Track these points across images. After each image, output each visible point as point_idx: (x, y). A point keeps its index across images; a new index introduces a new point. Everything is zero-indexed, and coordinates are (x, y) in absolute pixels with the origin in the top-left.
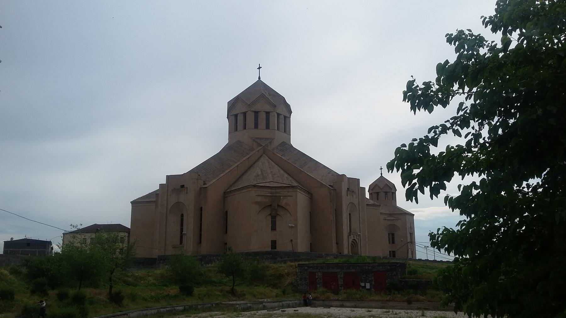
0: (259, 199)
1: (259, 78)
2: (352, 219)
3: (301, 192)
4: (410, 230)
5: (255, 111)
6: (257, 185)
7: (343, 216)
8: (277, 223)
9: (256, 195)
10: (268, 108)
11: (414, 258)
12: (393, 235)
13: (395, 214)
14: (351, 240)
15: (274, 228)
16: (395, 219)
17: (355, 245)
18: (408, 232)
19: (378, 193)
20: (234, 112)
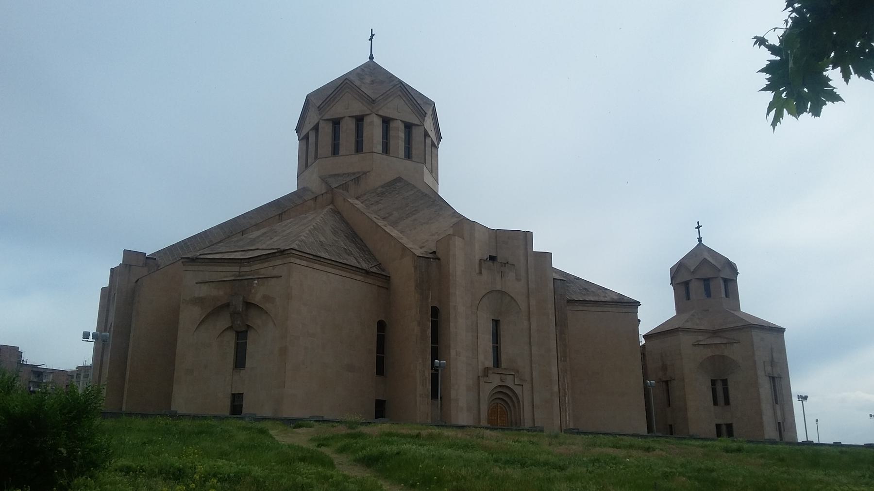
0: (204, 291)
1: (371, 58)
2: (503, 333)
3: (316, 266)
4: (769, 369)
5: (335, 119)
6: (202, 257)
7: (452, 324)
8: (250, 348)
9: (197, 283)
10: (358, 108)
11: (787, 438)
12: (725, 382)
13: (723, 331)
14: (487, 389)
15: (240, 362)
16: (725, 341)
17: (512, 401)
18: (761, 373)
19: (686, 284)
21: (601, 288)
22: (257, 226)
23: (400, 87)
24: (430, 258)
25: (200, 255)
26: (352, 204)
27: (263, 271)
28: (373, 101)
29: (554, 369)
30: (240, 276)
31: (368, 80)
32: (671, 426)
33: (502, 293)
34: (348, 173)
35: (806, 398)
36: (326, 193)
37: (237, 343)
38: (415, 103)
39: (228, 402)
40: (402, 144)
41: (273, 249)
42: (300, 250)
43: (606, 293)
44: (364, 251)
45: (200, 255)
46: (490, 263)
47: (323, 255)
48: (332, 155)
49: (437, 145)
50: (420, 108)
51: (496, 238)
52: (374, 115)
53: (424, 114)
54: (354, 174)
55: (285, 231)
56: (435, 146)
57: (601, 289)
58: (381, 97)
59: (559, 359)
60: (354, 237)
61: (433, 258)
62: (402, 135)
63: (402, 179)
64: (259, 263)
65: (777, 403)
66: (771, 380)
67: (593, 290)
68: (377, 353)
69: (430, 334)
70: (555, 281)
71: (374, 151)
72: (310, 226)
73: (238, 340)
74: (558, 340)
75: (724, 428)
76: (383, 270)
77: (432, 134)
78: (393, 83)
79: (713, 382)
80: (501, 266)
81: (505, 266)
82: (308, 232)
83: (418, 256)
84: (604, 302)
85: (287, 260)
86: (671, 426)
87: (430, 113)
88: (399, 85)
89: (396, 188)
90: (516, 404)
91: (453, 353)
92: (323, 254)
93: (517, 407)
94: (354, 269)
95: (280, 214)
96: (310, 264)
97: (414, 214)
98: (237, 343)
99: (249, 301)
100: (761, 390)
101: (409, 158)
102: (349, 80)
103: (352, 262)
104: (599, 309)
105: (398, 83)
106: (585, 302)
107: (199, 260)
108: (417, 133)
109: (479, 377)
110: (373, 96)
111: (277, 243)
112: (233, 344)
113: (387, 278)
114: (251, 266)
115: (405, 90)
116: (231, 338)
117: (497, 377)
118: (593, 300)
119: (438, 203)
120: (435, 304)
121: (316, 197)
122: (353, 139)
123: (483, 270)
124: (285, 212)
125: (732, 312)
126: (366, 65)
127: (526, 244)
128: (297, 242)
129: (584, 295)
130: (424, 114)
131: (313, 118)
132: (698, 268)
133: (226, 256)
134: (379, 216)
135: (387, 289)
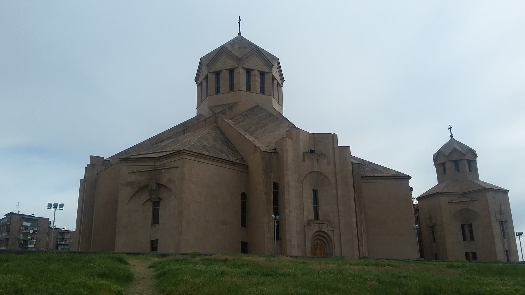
0: (133, 178)
1: (240, 34)
3: (200, 160)
4: (499, 216)
5: (217, 71)
7: (286, 193)
8: (161, 212)
9: (129, 173)
10: (230, 64)
12: (470, 226)
13: (468, 193)
14: (310, 233)
15: (155, 221)
18: (493, 219)
19: (444, 164)
20: (200, 81)
21: (385, 168)
22: (169, 138)
23: (256, 49)
24: (272, 152)
25: (131, 156)
26: (226, 122)
27: (167, 164)
28: (240, 59)
29: (354, 220)
30: (154, 168)
31: (237, 47)
32: (436, 254)
33: (319, 173)
34: (225, 104)
35: (522, 234)
36: (212, 116)
37: (154, 209)
38: (267, 60)
39: (149, 245)
40: (258, 85)
41: (174, 151)
42: (189, 150)
43: (389, 171)
44: (233, 150)
45: (131, 156)
46: (310, 154)
47: (205, 153)
48: (216, 93)
49: (281, 85)
50: (269, 62)
51: (314, 138)
52: (240, 67)
53: (272, 65)
54: (229, 104)
55: (184, 140)
56: (280, 86)
57: (385, 169)
58: (244, 57)
59: (357, 214)
60: (227, 142)
61: (273, 152)
62: (258, 79)
63: (259, 106)
64: (165, 160)
65: (505, 238)
66: (501, 223)
67: (380, 170)
68: (241, 213)
69: (273, 200)
70: (353, 164)
71: (241, 89)
72: (199, 136)
73: (154, 207)
74: (356, 201)
75: (471, 256)
76: (244, 162)
77: (278, 78)
78: (251, 48)
79: (463, 226)
80: (317, 156)
81: (320, 156)
82: (197, 140)
83: (264, 151)
84: (387, 177)
85: (182, 157)
86: (436, 254)
87: (275, 65)
88: (256, 49)
89: (254, 112)
90: (330, 242)
91: (287, 211)
92: (205, 153)
93: (330, 244)
94: (225, 161)
95: (183, 131)
96: (197, 159)
97: (265, 127)
98: (154, 209)
99: (160, 183)
100: (494, 230)
101: (263, 93)
102: (225, 48)
103: (224, 157)
104: (384, 181)
105: (254, 47)
106: (374, 177)
107: (130, 159)
108: (268, 78)
109: (304, 226)
110: (239, 56)
111: (178, 147)
112: (151, 209)
113: (247, 166)
114: (161, 161)
115: (259, 51)
116: (150, 205)
117: (317, 225)
118: (380, 176)
119: (280, 119)
120: (276, 181)
121: (206, 120)
122: (228, 83)
123: (306, 159)
124: (186, 129)
125: (474, 181)
126: (236, 38)
127: (333, 142)
128: (188, 146)
129: (374, 173)
130: (272, 65)
131: (204, 72)
132: (450, 153)
133: (146, 156)
134: (243, 129)
135: (247, 173)
